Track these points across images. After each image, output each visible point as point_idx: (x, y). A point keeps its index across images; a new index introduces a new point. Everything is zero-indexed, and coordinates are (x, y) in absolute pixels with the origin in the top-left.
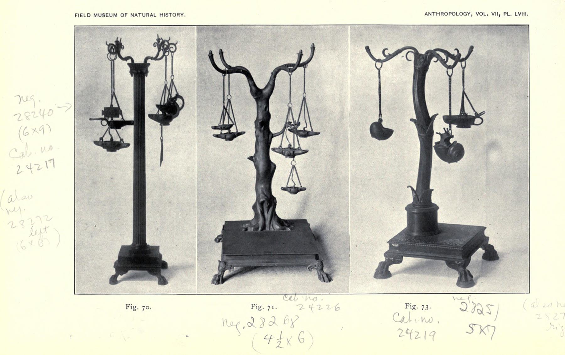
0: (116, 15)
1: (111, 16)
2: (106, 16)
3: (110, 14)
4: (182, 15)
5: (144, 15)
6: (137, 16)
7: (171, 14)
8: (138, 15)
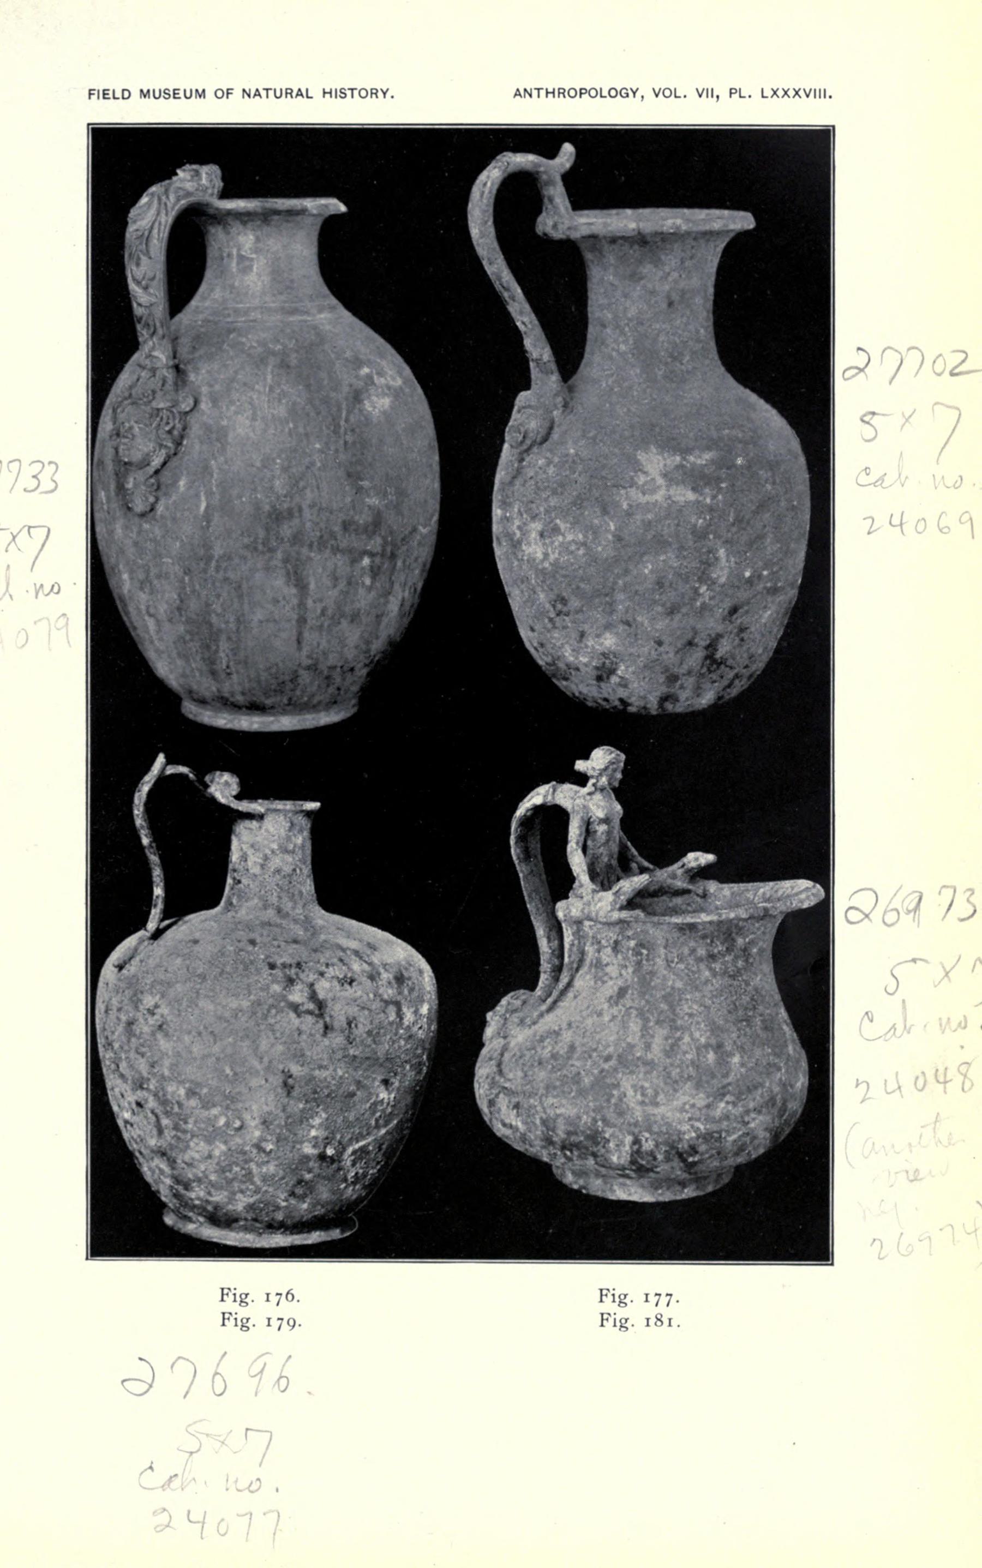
0: (201, 94)
1: (188, 95)
2: (175, 98)
3: (185, 91)
4: (385, 94)
5: (278, 95)
6: (259, 95)
8: (263, 93)
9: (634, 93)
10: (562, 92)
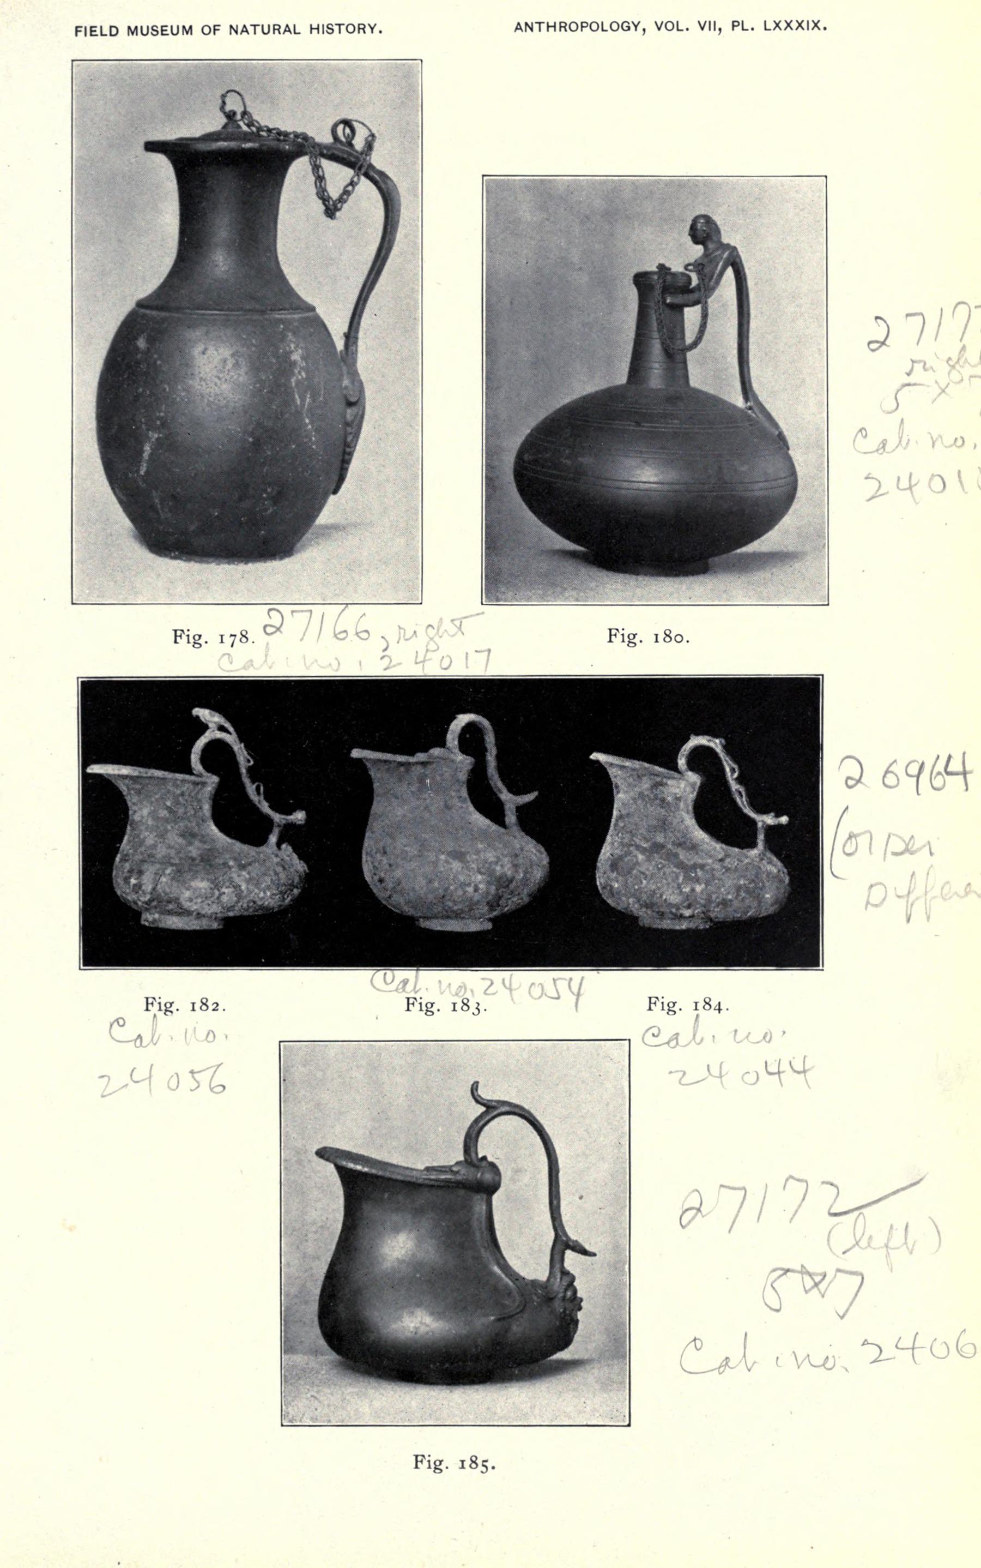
0: (188, 30)
1: (175, 31)
2: (162, 34)
3: (172, 27)
5: (266, 31)
6: (247, 31)
7: (342, 27)
8: (251, 29)
9: (636, 27)
10: (563, 26)
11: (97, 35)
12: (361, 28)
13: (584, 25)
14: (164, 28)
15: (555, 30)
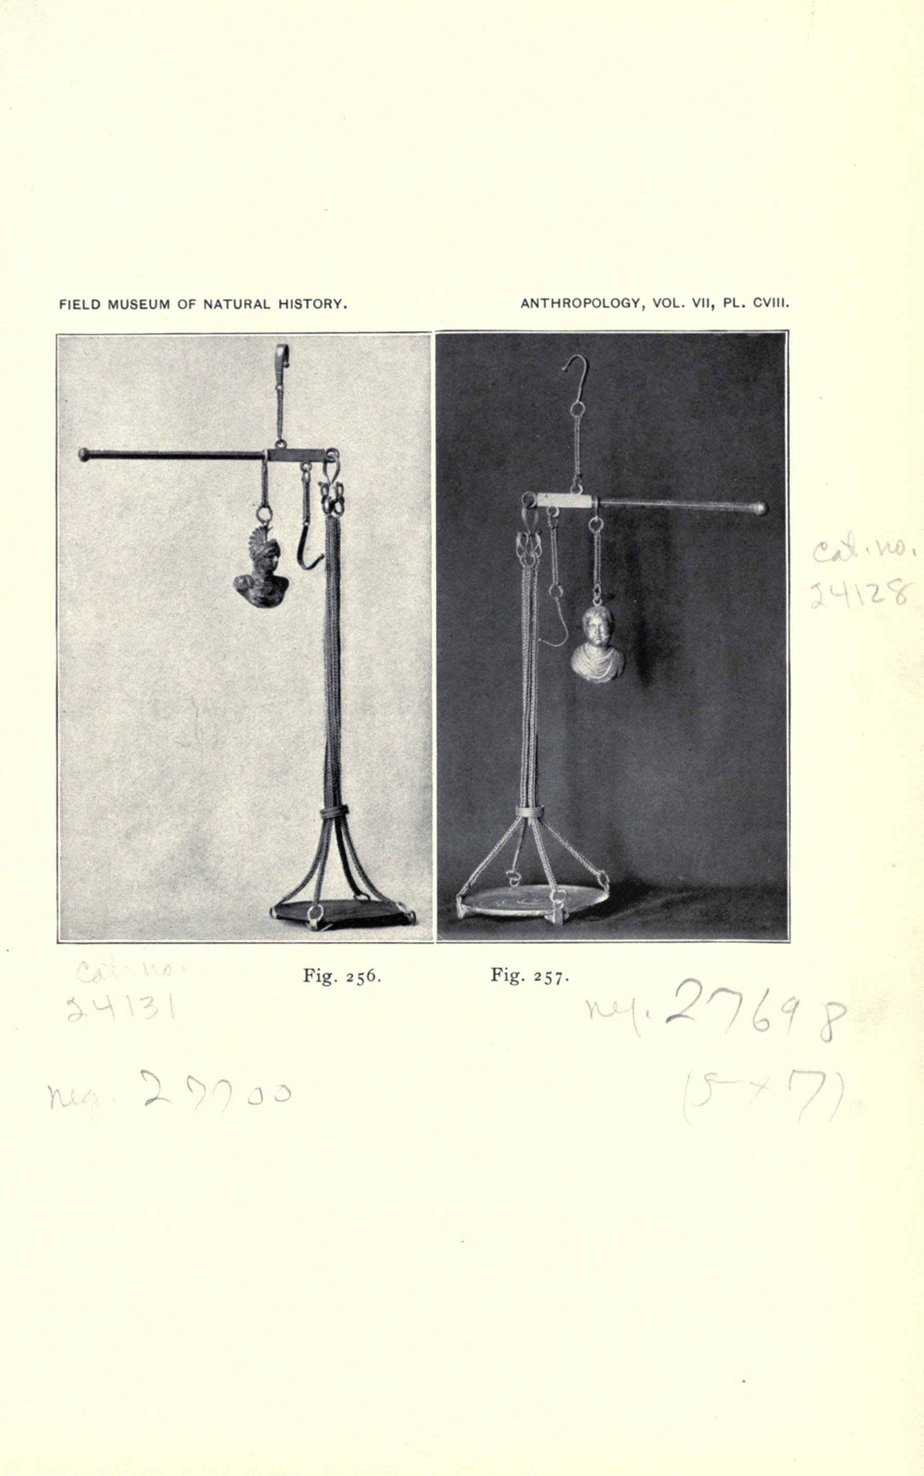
0: (166, 304)
1: (153, 305)
2: (141, 308)
3: (150, 301)
5: (238, 305)
6: (220, 306)
7: (310, 302)
8: (224, 304)
9: (636, 303)
10: (567, 302)
11: (79, 308)
12: (327, 303)
13: (587, 301)
14: (143, 302)
15: (559, 306)
